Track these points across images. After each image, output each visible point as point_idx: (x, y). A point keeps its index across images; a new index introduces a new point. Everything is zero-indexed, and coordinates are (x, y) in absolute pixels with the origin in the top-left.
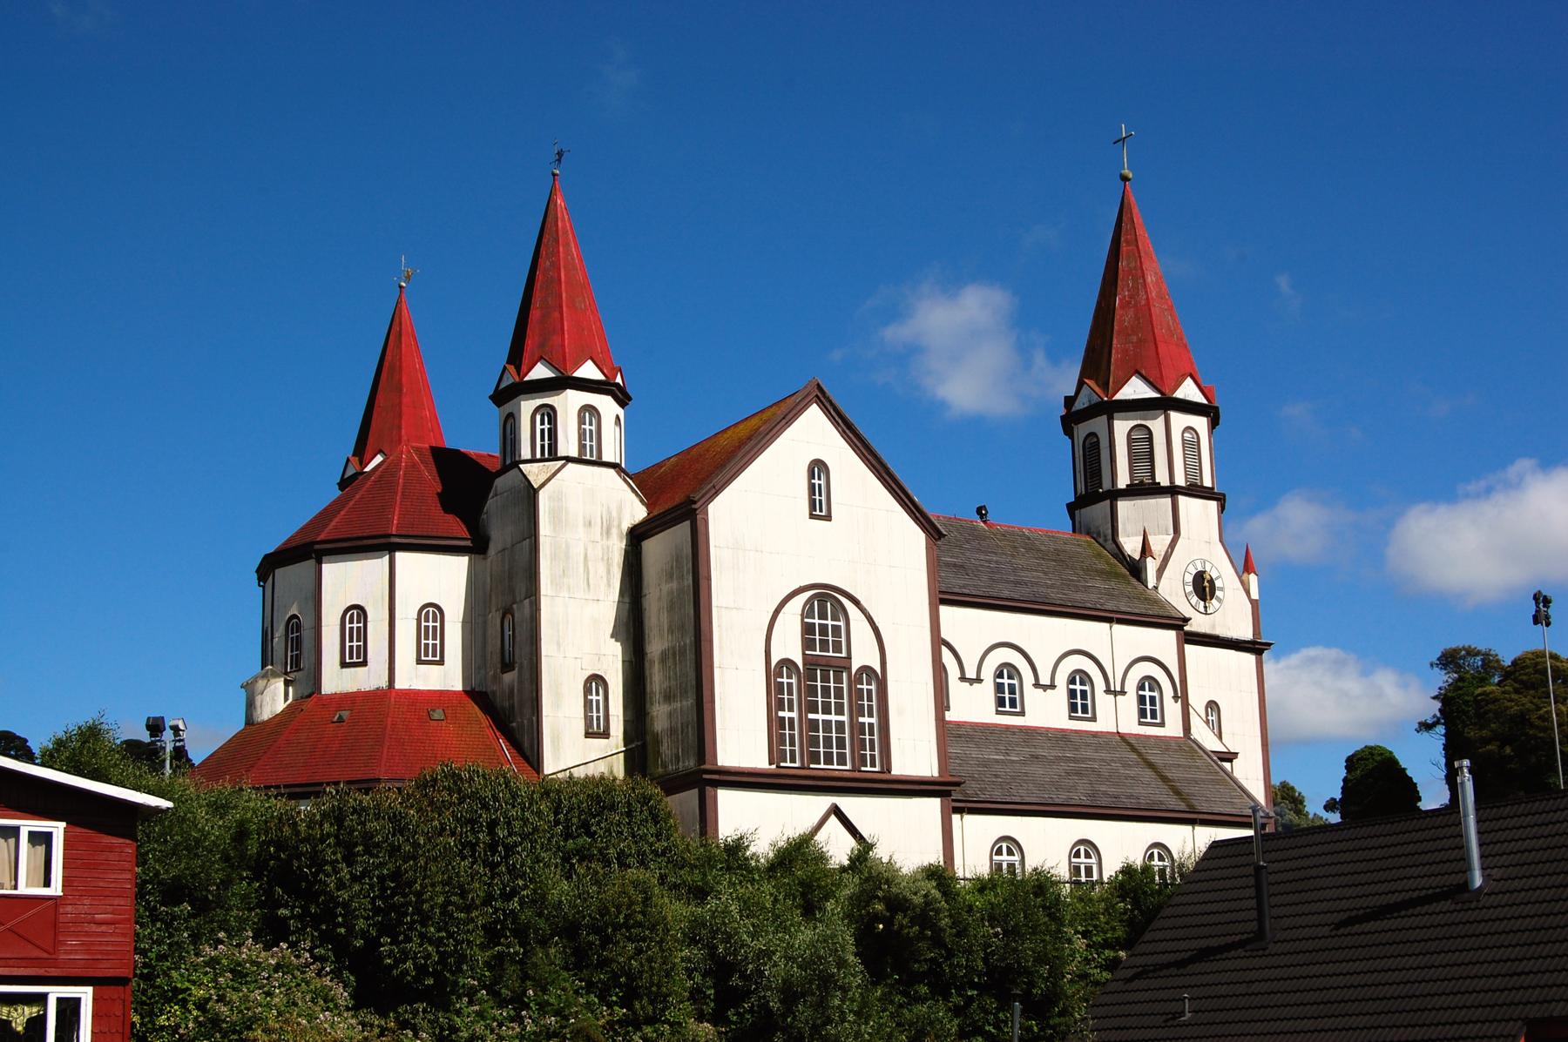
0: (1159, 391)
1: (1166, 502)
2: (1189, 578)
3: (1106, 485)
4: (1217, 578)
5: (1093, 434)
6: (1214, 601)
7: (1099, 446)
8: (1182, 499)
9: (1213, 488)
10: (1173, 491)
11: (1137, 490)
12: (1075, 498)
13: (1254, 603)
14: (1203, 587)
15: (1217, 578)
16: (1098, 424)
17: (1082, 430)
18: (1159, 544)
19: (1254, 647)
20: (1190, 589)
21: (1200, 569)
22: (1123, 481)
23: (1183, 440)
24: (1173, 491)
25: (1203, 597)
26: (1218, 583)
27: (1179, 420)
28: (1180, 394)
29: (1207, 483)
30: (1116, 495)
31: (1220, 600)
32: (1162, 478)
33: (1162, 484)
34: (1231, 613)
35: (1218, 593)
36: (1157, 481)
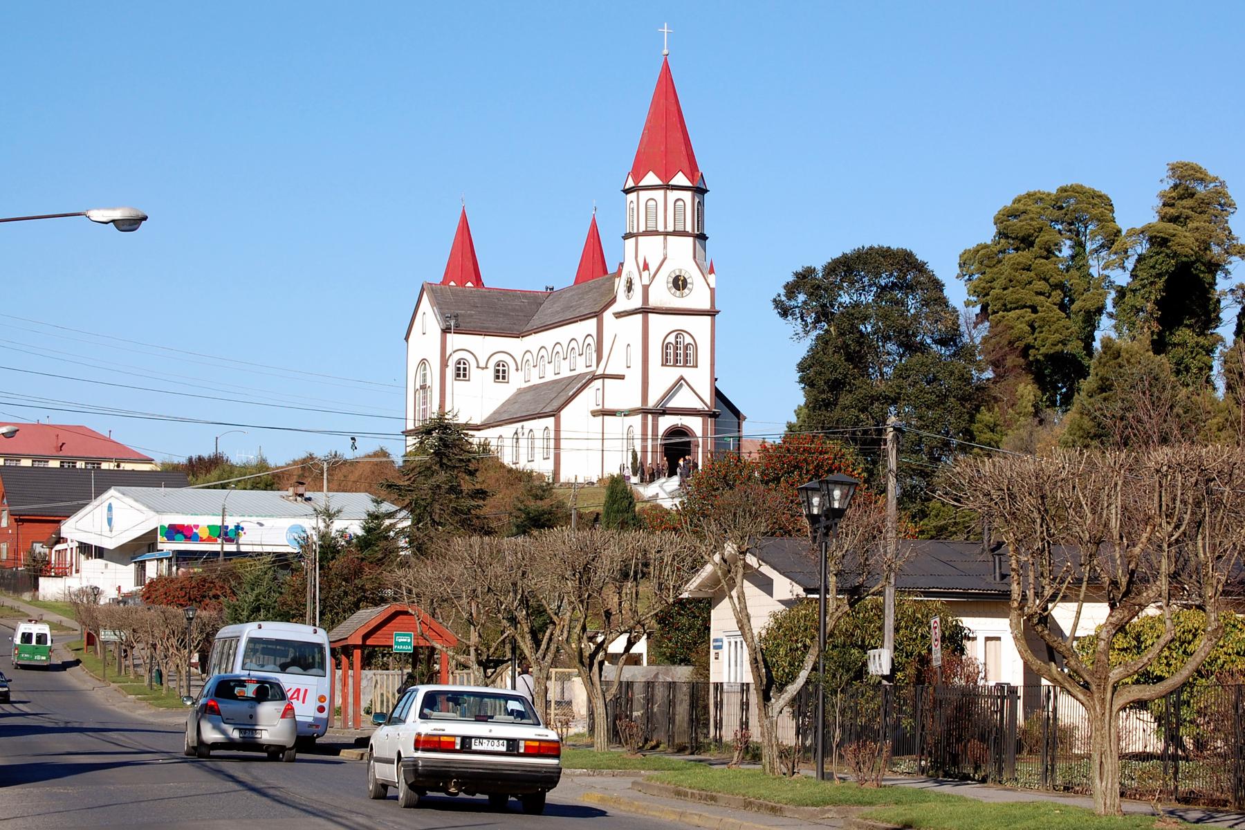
1: (662, 237)
2: (671, 280)
6: (686, 290)
10: (666, 234)
11: (647, 233)
13: (712, 290)
14: (679, 283)
16: (632, 196)
19: (712, 313)
21: (678, 274)
22: (642, 229)
24: (666, 234)
25: (685, 286)
26: (689, 281)
27: (673, 195)
28: (673, 182)
29: (689, 229)
30: (636, 235)
31: (689, 289)
34: (698, 297)
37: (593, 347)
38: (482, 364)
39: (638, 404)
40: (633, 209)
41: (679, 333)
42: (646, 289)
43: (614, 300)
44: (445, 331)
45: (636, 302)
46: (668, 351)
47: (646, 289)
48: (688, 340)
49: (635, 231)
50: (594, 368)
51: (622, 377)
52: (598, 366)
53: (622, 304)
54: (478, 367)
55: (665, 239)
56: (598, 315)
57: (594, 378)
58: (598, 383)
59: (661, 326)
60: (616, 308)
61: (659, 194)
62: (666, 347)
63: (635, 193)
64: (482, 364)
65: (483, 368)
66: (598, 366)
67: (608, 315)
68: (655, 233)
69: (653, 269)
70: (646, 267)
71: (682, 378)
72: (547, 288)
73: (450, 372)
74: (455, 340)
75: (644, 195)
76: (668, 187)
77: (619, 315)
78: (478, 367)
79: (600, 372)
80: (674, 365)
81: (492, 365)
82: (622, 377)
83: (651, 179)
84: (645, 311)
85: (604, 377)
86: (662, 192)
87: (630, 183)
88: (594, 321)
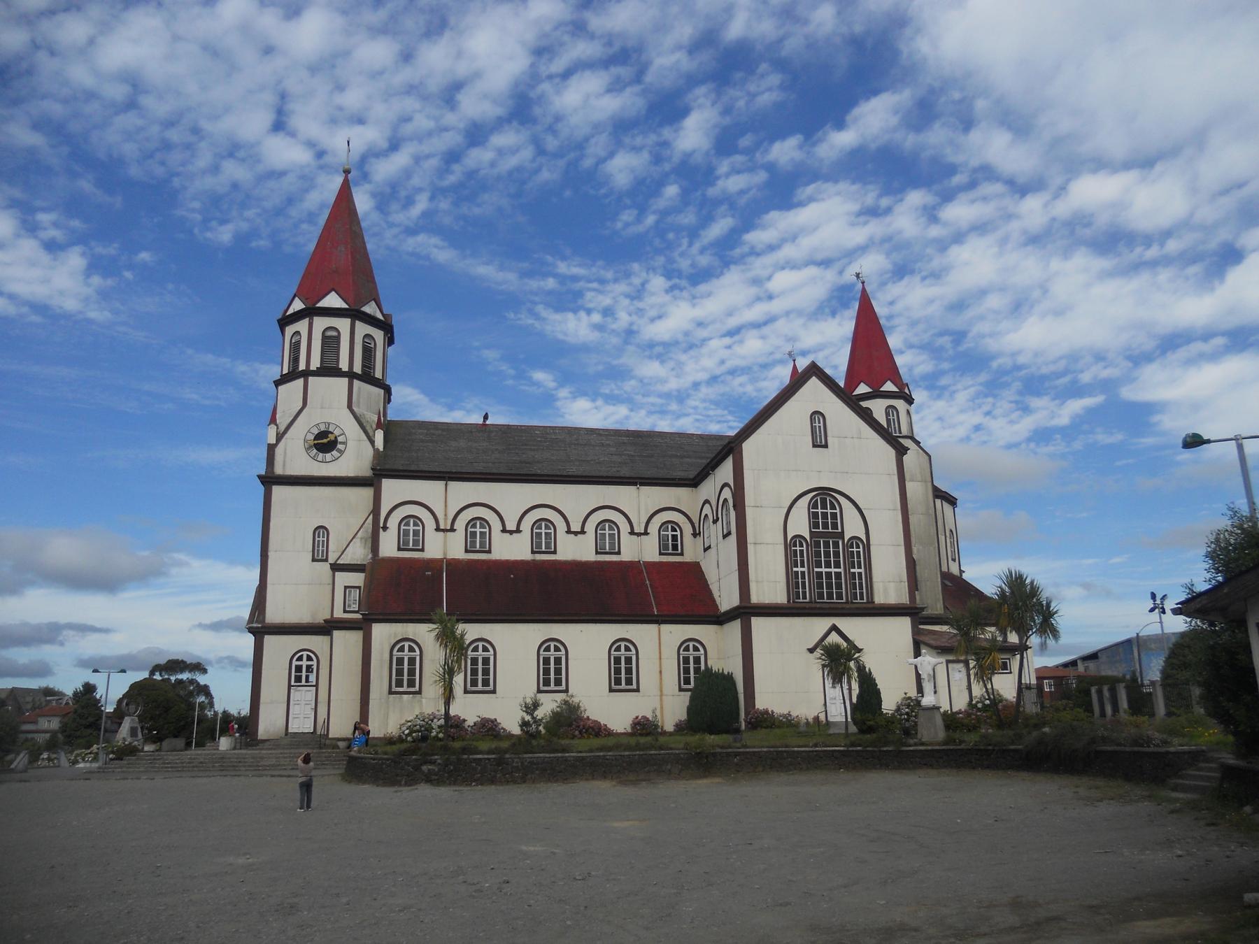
1: (346, 380)
3: (302, 366)
5: (297, 333)
8: (356, 383)
10: (351, 375)
23: (364, 342)
27: (362, 329)
29: (378, 374)
30: (307, 374)
32: (344, 366)
33: (343, 370)
61: (343, 324)
63: (306, 321)
75: (320, 323)
76: (354, 314)
83: (333, 301)
86: (347, 322)
87: (298, 305)
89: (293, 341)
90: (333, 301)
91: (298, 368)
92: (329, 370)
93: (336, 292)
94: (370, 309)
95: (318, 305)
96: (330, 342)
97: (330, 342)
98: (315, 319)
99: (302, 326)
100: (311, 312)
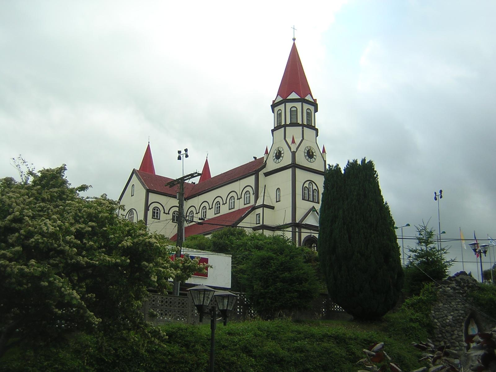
0: (300, 97)
2: (306, 151)
3: (283, 123)
4: (314, 152)
5: (280, 110)
7: (281, 115)
9: (315, 126)
10: (303, 125)
12: (274, 127)
15: (314, 152)
17: (276, 109)
18: (297, 141)
20: (306, 154)
23: (307, 112)
26: (314, 154)
27: (306, 106)
29: (313, 125)
30: (285, 126)
31: (315, 159)
32: (300, 122)
35: (314, 157)
36: (298, 122)
37: (251, 192)
38: (167, 212)
39: (289, 220)
40: (281, 113)
41: (311, 182)
42: (294, 154)
43: (264, 166)
44: (148, 191)
45: (287, 160)
46: (305, 192)
47: (294, 154)
48: (315, 187)
49: (283, 123)
50: (252, 203)
51: (273, 208)
52: (256, 202)
53: (272, 165)
54: (164, 213)
55: (303, 128)
56: (256, 173)
57: (254, 208)
58: (260, 211)
59: (302, 176)
60: (265, 171)
61: (298, 105)
62: (304, 189)
63: (284, 104)
64: (167, 212)
65: (166, 214)
66: (256, 202)
67: (261, 174)
68: (297, 125)
69: (297, 141)
70: (293, 142)
71: (314, 207)
72: (192, 183)
73: (150, 213)
74: (153, 197)
75: (289, 105)
76: (303, 100)
77: (267, 174)
78: (164, 213)
79: (260, 202)
80: (308, 200)
81: (171, 212)
82: (273, 208)
83: (294, 96)
84: (294, 166)
85: (264, 206)
87: (280, 99)
88: (253, 177)
89: (278, 113)
90: (294, 96)
91: (281, 124)
92: (294, 124)
93: (294, 92)
94: (308, 98)
95: (288, 98)
96: (293, 113)
97: (293, 113)
98: (287, 103)
99: (282, 107)
100: (285, 101)
